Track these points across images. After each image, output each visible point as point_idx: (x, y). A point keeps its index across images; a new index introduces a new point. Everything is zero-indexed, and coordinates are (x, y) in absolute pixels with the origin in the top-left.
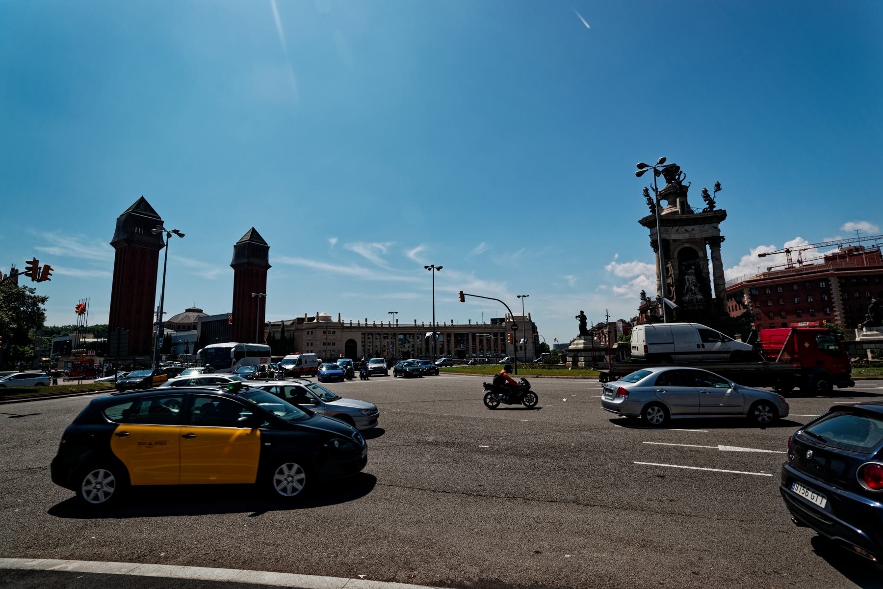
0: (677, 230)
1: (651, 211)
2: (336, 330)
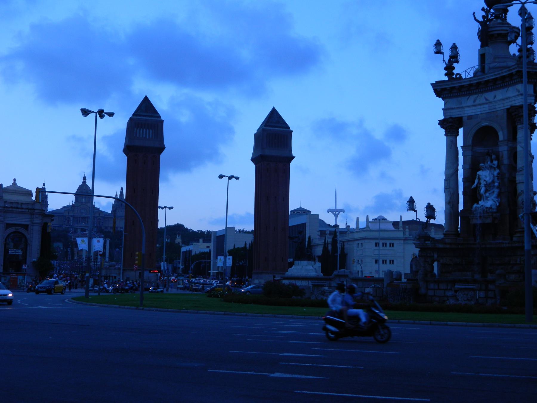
0: (475, 101)
1: (446, 75)
2: (395, 242)
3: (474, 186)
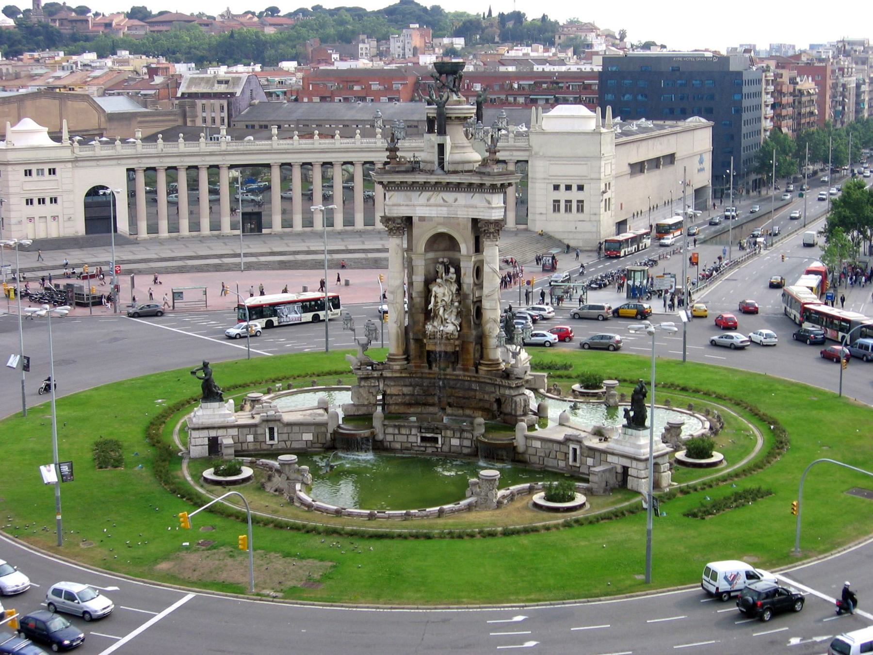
0: (428, 200)
3: (431, 306)
